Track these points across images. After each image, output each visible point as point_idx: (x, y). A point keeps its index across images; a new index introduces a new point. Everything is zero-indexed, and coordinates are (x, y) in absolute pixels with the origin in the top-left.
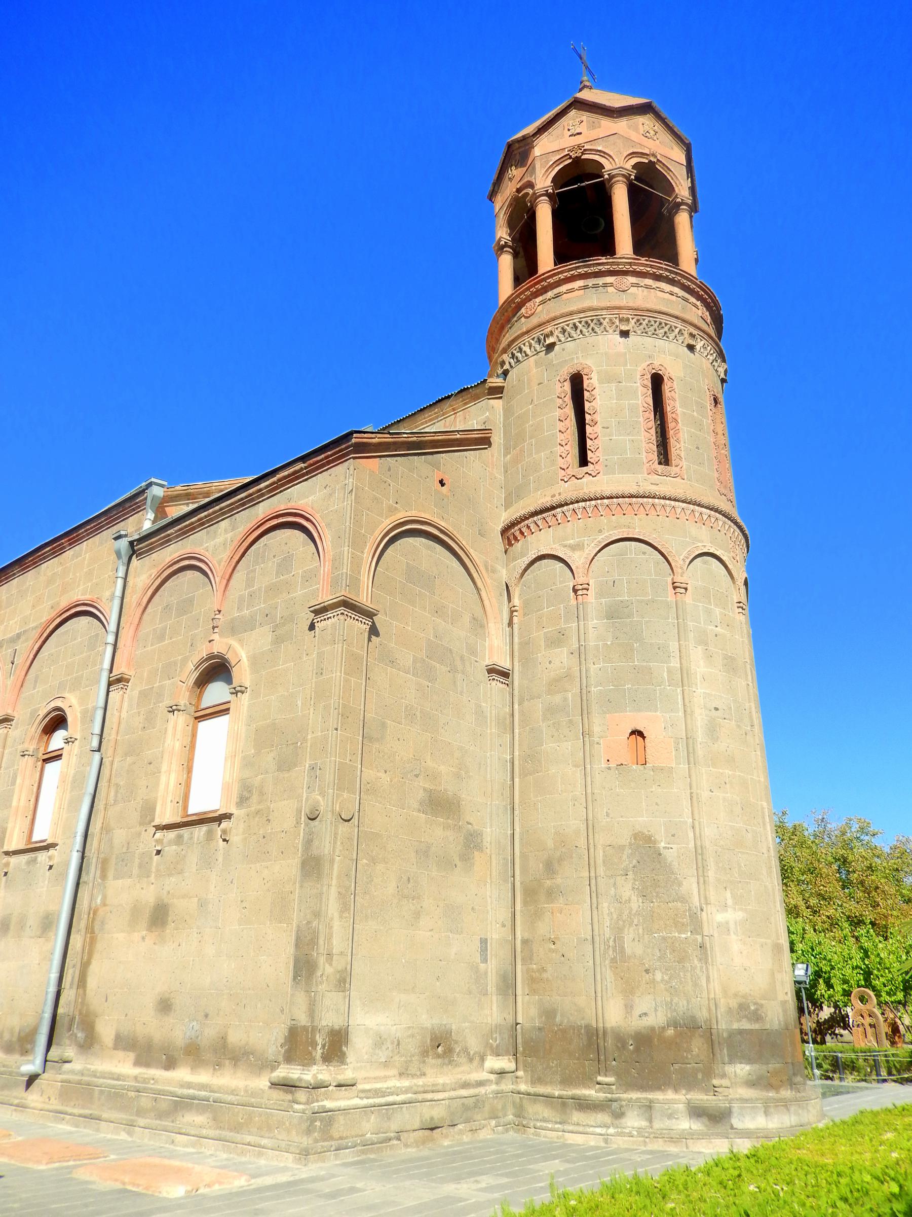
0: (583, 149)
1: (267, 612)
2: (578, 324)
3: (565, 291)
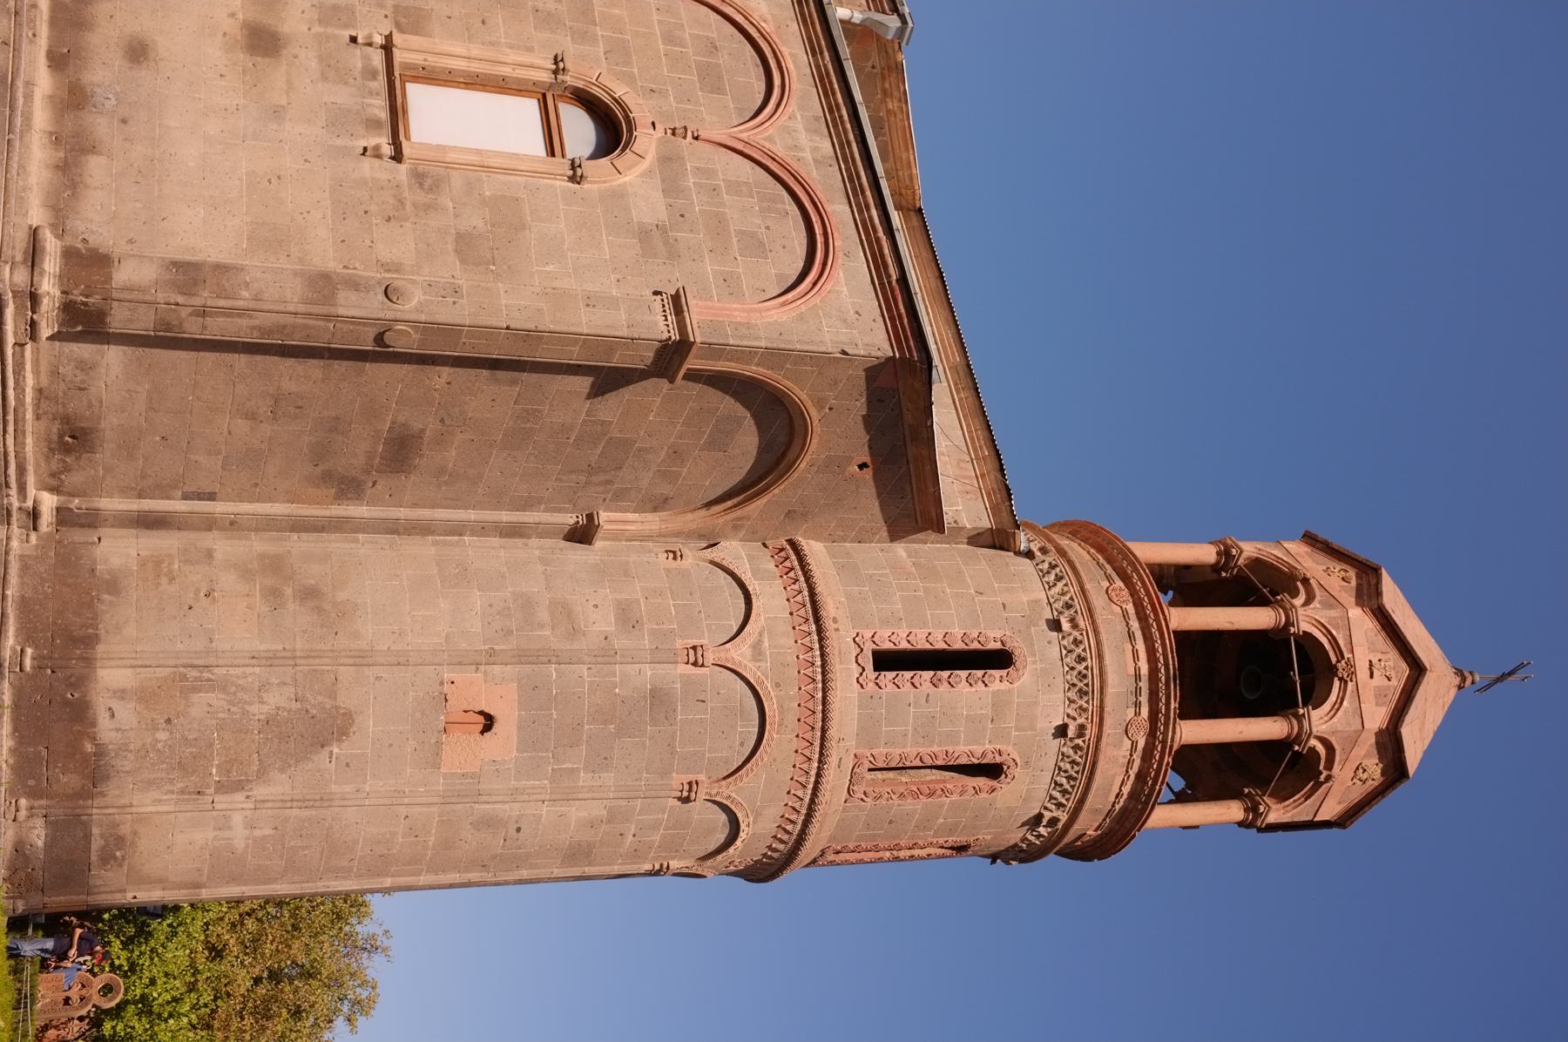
0: (1348, 679)
1: (687, 215)
2: (1084, 664)
3: (1136, 647)
